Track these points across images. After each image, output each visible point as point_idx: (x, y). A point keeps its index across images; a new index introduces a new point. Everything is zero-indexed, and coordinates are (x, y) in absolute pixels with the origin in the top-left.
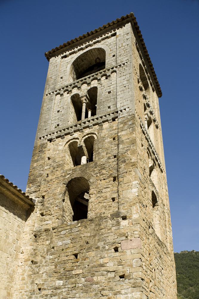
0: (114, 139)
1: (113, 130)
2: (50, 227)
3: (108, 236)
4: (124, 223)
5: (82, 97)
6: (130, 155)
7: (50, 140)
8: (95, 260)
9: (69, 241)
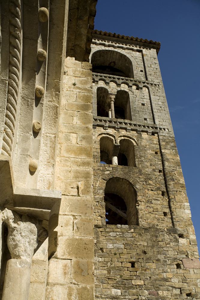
0: (156, 153)
1: (154, 144)
3: (168, 251)
4: (182, 241)
5: (111, 94)
6: (178, 175)
8: (157, 273)
9: (122, 246)
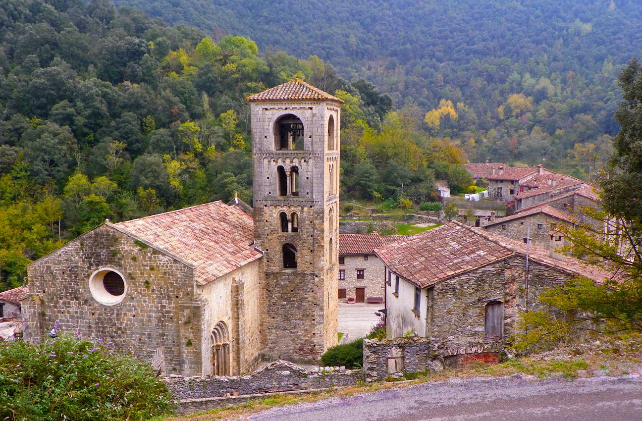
2: (275, 271)
4: (317, 279)
7: (266, 206)
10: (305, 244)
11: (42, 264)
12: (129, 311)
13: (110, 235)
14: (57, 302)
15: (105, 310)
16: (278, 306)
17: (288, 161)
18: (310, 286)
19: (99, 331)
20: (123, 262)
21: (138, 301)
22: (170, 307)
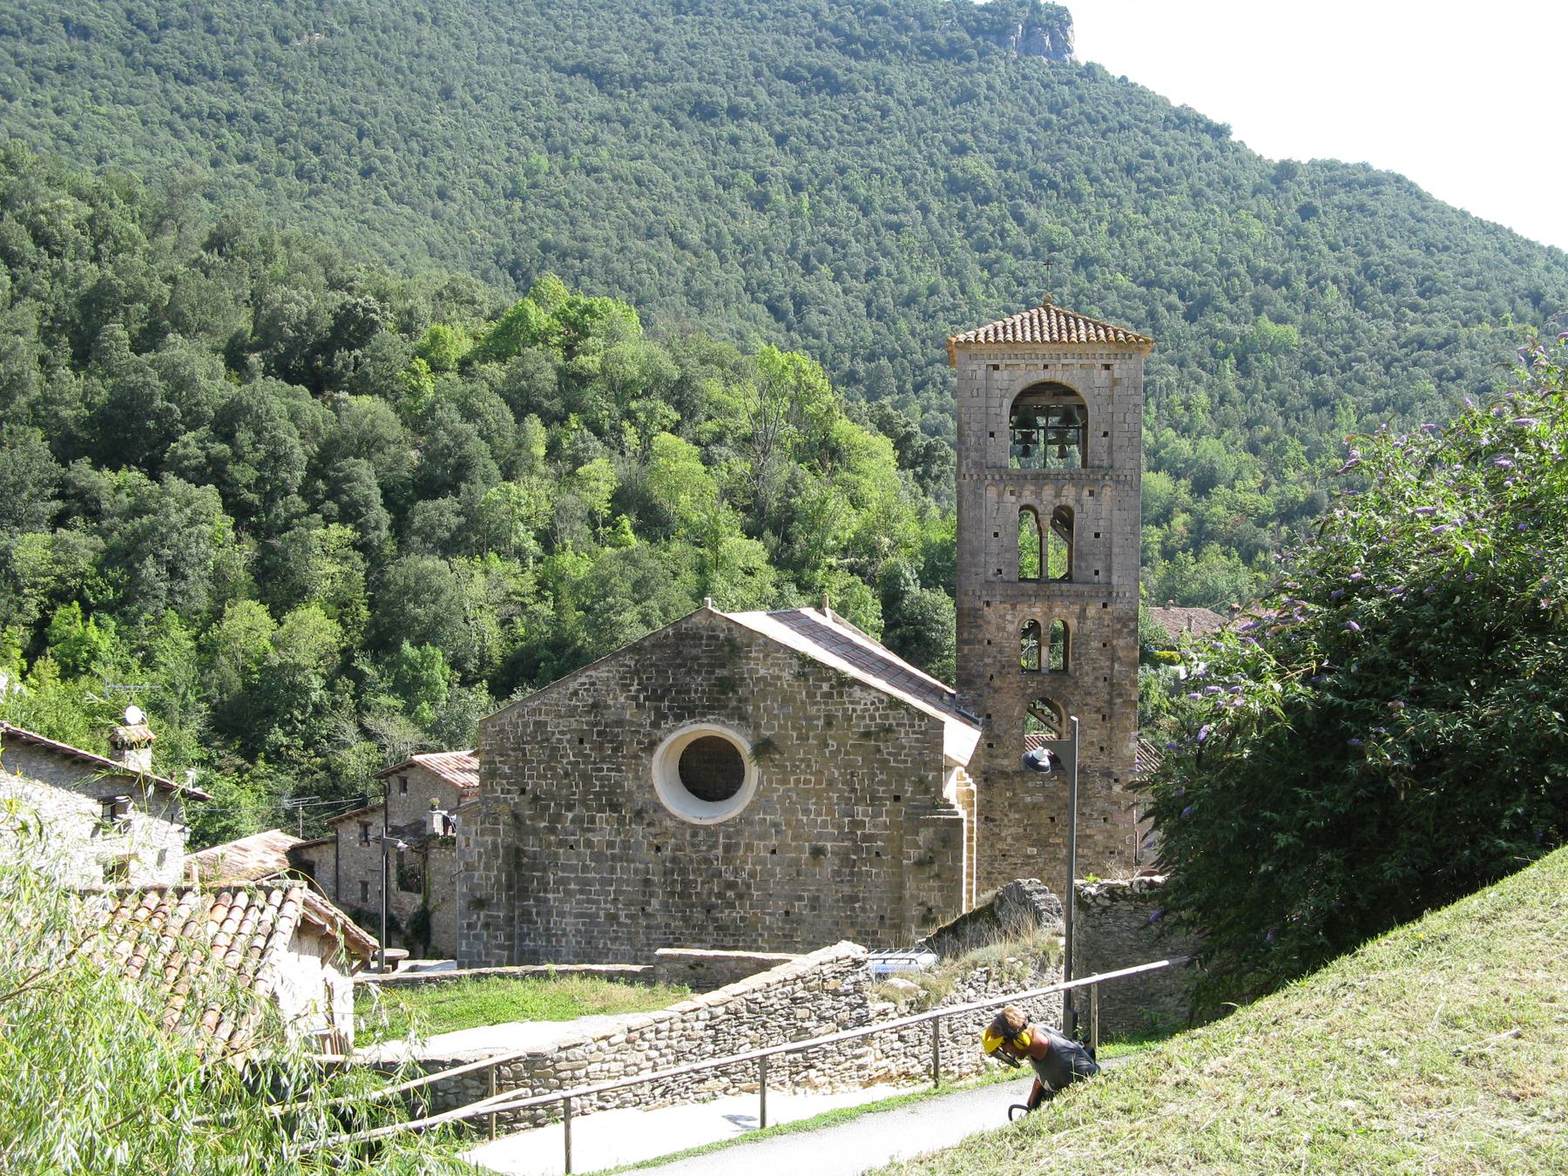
7: (988, 604)
10: (1089, 700)
11: (520, 716)
12: (761, 837)
13: (717, 638)
14: (557, 818)
15: (694, 835)
16: (1014, 860)
17: (1048, 492)
18: (1100, 804)
19: (672, 894)
20: (750, 708)
21: (785, 811)
22: (875, 826)
